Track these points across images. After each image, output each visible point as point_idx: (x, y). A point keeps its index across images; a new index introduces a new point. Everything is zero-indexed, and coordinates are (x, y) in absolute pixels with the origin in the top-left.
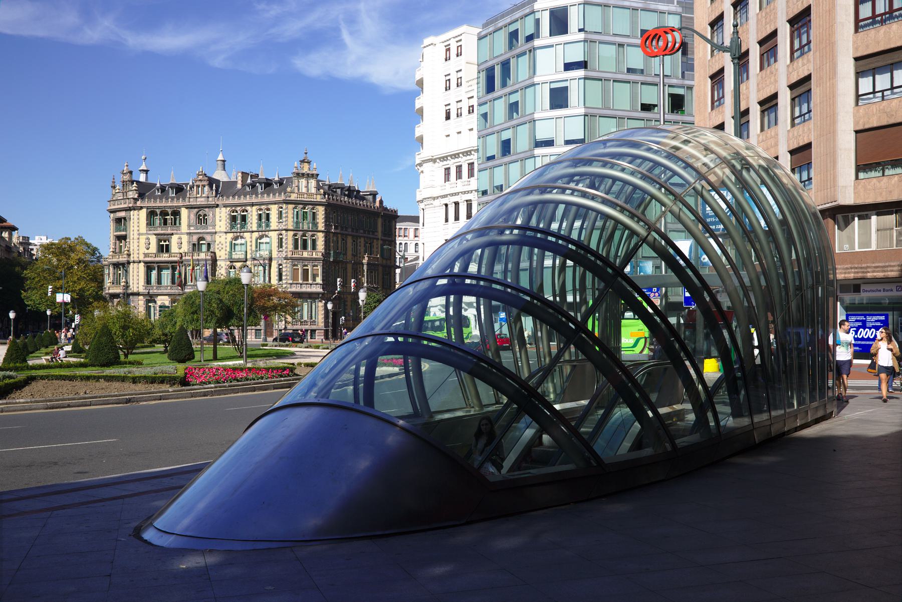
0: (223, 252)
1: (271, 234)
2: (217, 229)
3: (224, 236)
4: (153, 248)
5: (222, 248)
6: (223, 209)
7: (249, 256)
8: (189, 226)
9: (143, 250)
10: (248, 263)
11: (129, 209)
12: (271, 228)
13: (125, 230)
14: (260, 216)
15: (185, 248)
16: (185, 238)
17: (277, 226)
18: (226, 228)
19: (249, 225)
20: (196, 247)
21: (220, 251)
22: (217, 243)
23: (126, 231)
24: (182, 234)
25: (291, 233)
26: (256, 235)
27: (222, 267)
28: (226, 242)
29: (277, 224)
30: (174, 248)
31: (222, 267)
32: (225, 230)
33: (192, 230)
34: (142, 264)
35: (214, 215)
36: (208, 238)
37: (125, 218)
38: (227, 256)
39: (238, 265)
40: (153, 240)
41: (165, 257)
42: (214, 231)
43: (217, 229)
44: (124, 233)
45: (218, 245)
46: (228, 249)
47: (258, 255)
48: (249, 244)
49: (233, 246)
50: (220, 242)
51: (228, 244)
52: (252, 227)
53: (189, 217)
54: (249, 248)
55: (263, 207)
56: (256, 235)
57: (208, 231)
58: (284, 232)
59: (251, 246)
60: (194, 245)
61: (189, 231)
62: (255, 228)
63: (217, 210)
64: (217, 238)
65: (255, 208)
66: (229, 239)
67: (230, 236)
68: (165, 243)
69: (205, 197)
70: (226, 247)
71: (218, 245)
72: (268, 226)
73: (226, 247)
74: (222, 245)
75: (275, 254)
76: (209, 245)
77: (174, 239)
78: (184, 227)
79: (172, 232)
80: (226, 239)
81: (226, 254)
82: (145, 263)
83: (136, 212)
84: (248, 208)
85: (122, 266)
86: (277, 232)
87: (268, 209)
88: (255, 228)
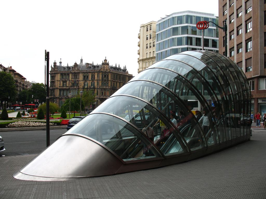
1: (95, 81)
4: (61, 85)
7: (89, 87)
8: (72, 79)
9: (59, 85)
10: (88, 89)
11: (55, 73)
13: (54, 80)
14: (92, 76)
15: (71, 84)
19: (89, 78)
22: (80, 83)
23: (54, 80)
25: (101, 81)
30: (68, 85)
34: (58, 90)
36: (77, 82)
37: (54, 76)
40: (62, 82)
41: (65, 88)
43: (80, 80)
44: (54, 80)
46: (83, 85)
48: (89, 84)
49: (85, 84)
54: (89, 85)
55: (93, 73)
56: (91, 81)
60: (73, 84)
67: (84, 81)
72: (94, 78)
75: (96, 87)
76: (77, 84)
77: (68, 82)
78: (70, 79)
82: (59, 89)
83: (57, 74)
84: (89, 74)
85: (53, 90)
87: (94, 74)
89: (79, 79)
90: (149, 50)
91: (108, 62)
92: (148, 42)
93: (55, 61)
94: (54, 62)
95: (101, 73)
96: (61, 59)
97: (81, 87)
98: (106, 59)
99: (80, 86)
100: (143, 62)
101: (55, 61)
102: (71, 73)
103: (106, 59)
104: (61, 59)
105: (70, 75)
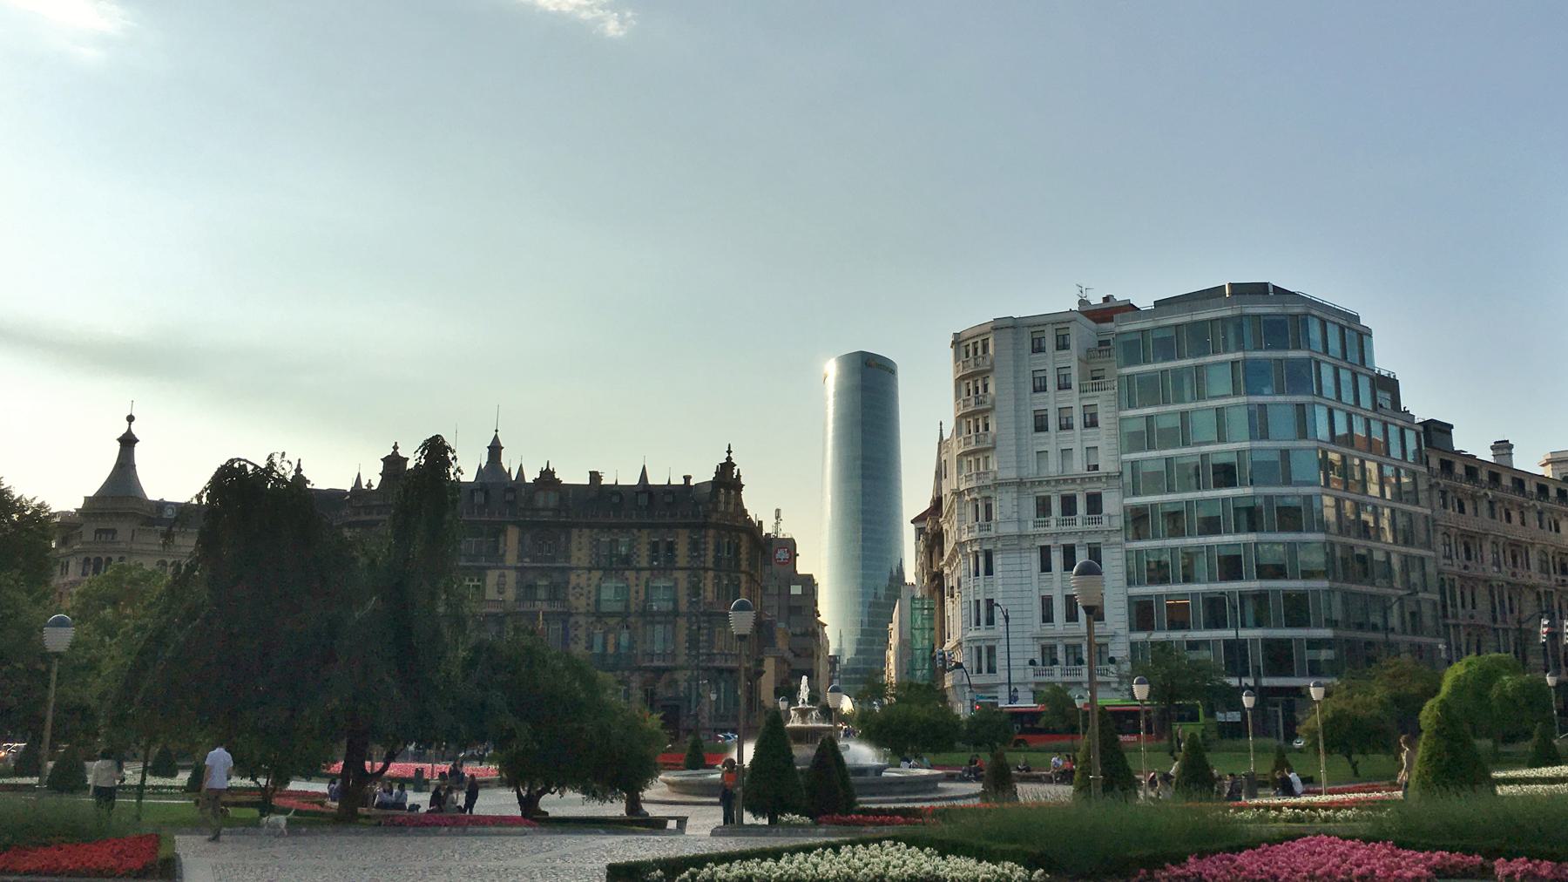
0: (583, 601)
1: (678, 574)
2: (574, 562)
3: (585, 577)
5: (582, 595)
6: (586, 531)
7: (633, 608)
8: (520, 558)
10: (632, 619)
12: (677, 565)
15: (510, 594)
16: (511, 577)
17: (688, 562)
18: (590, 562)
20: (528, 590)
21: (577, 598)
24: (509, 568)
25: (711, 574)
26: (646, 574)
27: (580, 626)
28: (589, 586)
29: (689, 559)
30: (491, 593)
31: (580, 626)
32: (586, 565)
33: (527, 562)
35: (568, 540)
38: (592, 609)
39: (612, 622)
42: (567, 565)
43: (574, 562)
45: (574, 588)
47: (655, 608)
48: (634, 589)
50: (578, 585)
51: (592, 588)
52: (638, 562)
53: (520, 541)
54: (633, 594)
57: (558, 565)
58: (701, 572)
59: (637, 592)
61: (519, 565)
62: (644, 564)
63: (575, 532)
64: (573, 578)
65: (645, 532)
66: (595, 581)
67: (597, 574)
68: (471, 584)
69: (551, 510)
70: (589, 592)
71: (574, 588)
73: (589, 592)
74: (582, 588)
75: (683, 606)
77: (492, 577)
78: (511, 559)
79: (485, 564)
80: (589, 579)
81: (588, 605)
86: (689, 572)
88: (644, 564)
89: (568, 558)
90: (1052, 440)
91: (739, 476)
92: (1051, 402)
93: (395, 447)
94: (390, 452)
95: (711, 532)
96: (130, 419)
97: (581, 604)
98: (729, 459)
99: (571, 598)
100: (1018, 492)
101: (395, 447)
102: (514, 523)
103: (729, 459)
104: (130, 419)
105: (513, 535)
